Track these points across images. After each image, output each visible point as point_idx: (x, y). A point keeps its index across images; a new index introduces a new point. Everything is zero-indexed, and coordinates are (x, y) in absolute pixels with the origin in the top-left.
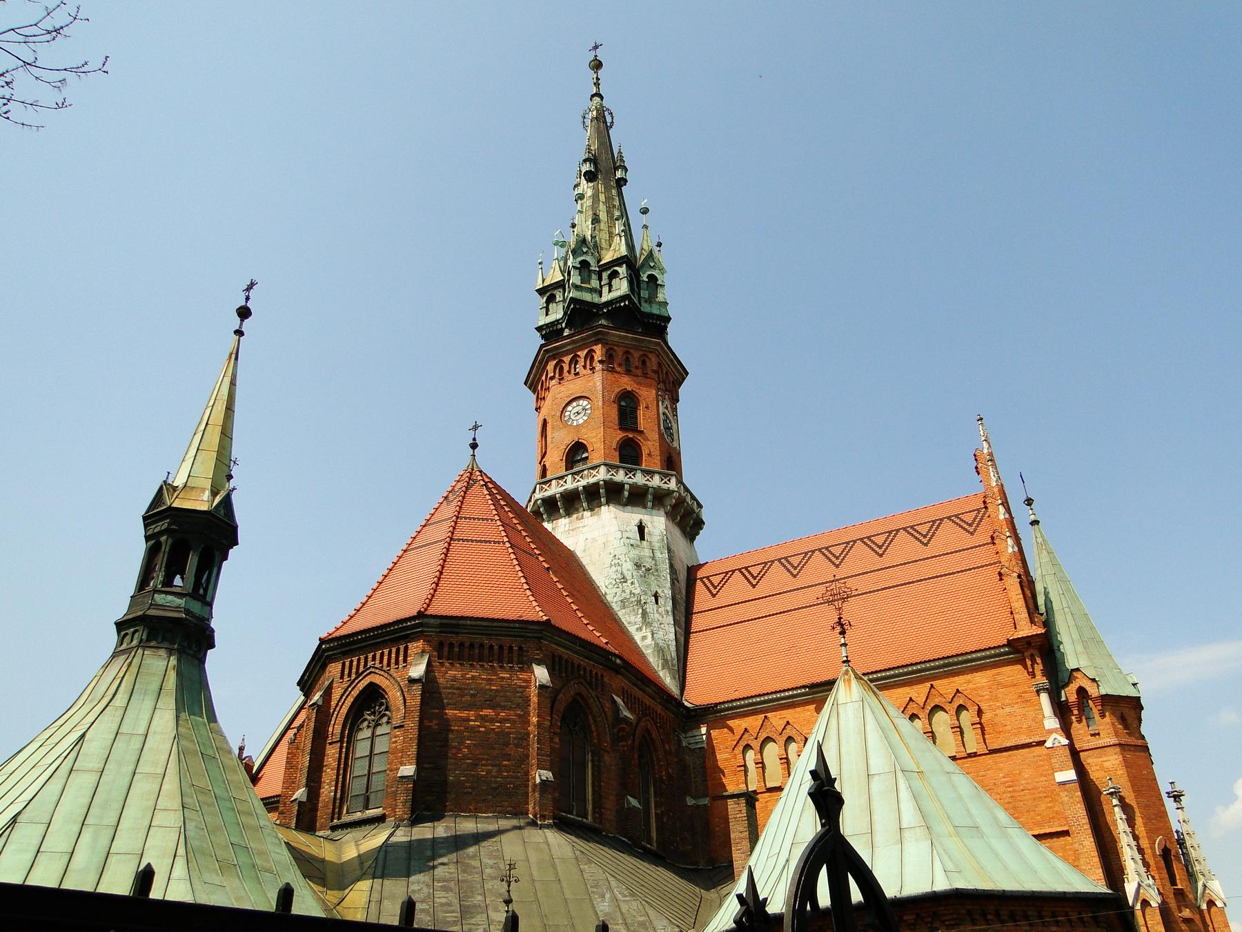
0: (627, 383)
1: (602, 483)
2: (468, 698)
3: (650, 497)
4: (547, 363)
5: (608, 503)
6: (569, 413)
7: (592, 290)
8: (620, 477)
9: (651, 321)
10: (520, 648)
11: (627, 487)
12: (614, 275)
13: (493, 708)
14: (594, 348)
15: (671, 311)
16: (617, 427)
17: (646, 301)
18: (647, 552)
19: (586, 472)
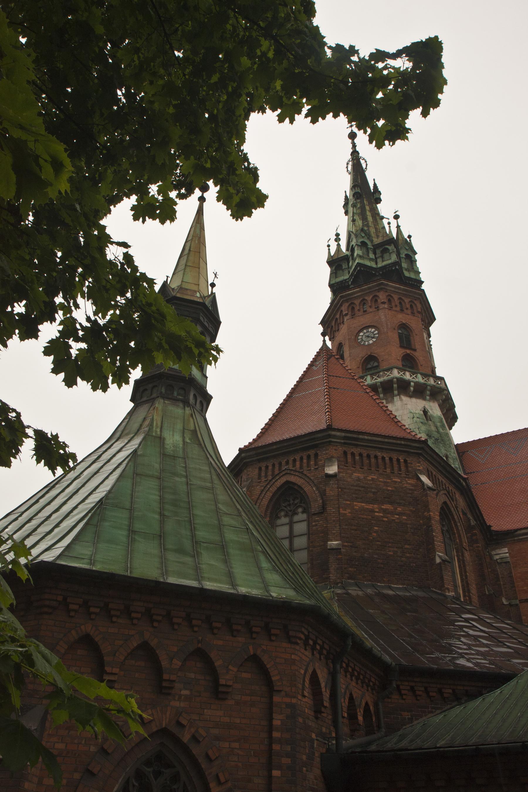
0: (402, 318)
1: (395, 380)
2: (371, 495)
3: (428, 393)
4: (341, 305)
5: (399, 394)
6: (361, 337)
7: (371, 260)
8: (407, 376)
9: (411, 282)
10: (405, 461)
11: (412, 384)
12: (386, 251)
13: (391, 503)
14: (377, 294)
15: (422, 277)
16: (398, 346)
17: (406, 270)
18: (433, 428)
19: (381, 373)
